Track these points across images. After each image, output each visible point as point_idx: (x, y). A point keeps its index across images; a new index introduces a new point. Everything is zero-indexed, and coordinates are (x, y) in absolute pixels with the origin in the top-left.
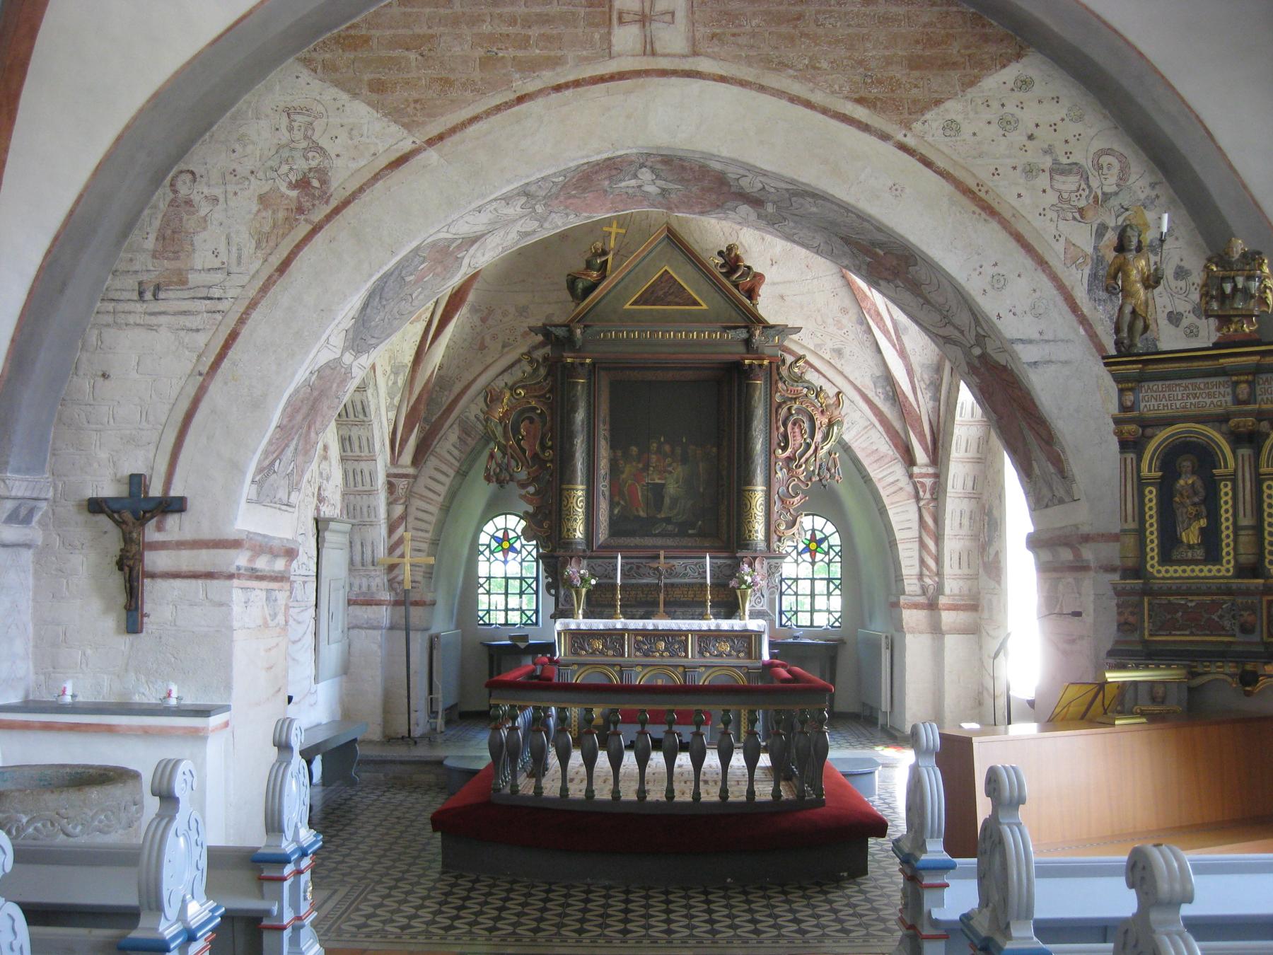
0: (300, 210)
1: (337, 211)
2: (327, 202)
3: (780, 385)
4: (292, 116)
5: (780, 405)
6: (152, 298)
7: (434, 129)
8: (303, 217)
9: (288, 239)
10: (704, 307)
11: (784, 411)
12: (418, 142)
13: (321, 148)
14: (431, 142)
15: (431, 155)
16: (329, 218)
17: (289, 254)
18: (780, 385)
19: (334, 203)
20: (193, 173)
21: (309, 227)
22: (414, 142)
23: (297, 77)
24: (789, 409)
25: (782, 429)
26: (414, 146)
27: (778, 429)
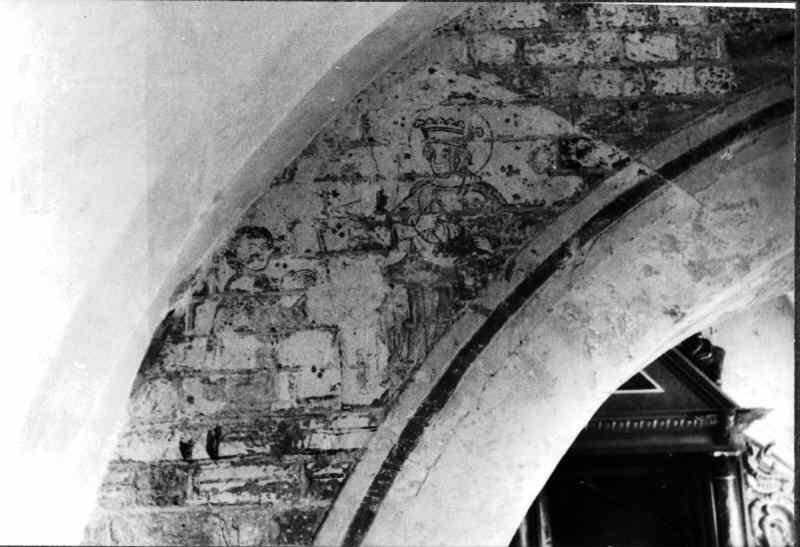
0: (462, 292)
1: (526, 290)
2: (508, 277)
3: (750, 479)
4: (432, 134)
5: (751, 505)
6: (206, 455)
7: (672, 148)
8: (468, 302)
9: (446, 343)
10: (659, 389)
11: (757, 514)
12: (648, 171)
13: (487, 186)
14: (673, 170)
15: (676, 196)
16: (515, 302)
17: (451, 368)
18: (750, 479)
19: (519, 278)
20: (264, 233)
21: (481, 320)
22: (641, 172)
23: (432, 71)
24: (764, 509)
25: (759, 532)
26: (642, 177)
27: (753, 532)
